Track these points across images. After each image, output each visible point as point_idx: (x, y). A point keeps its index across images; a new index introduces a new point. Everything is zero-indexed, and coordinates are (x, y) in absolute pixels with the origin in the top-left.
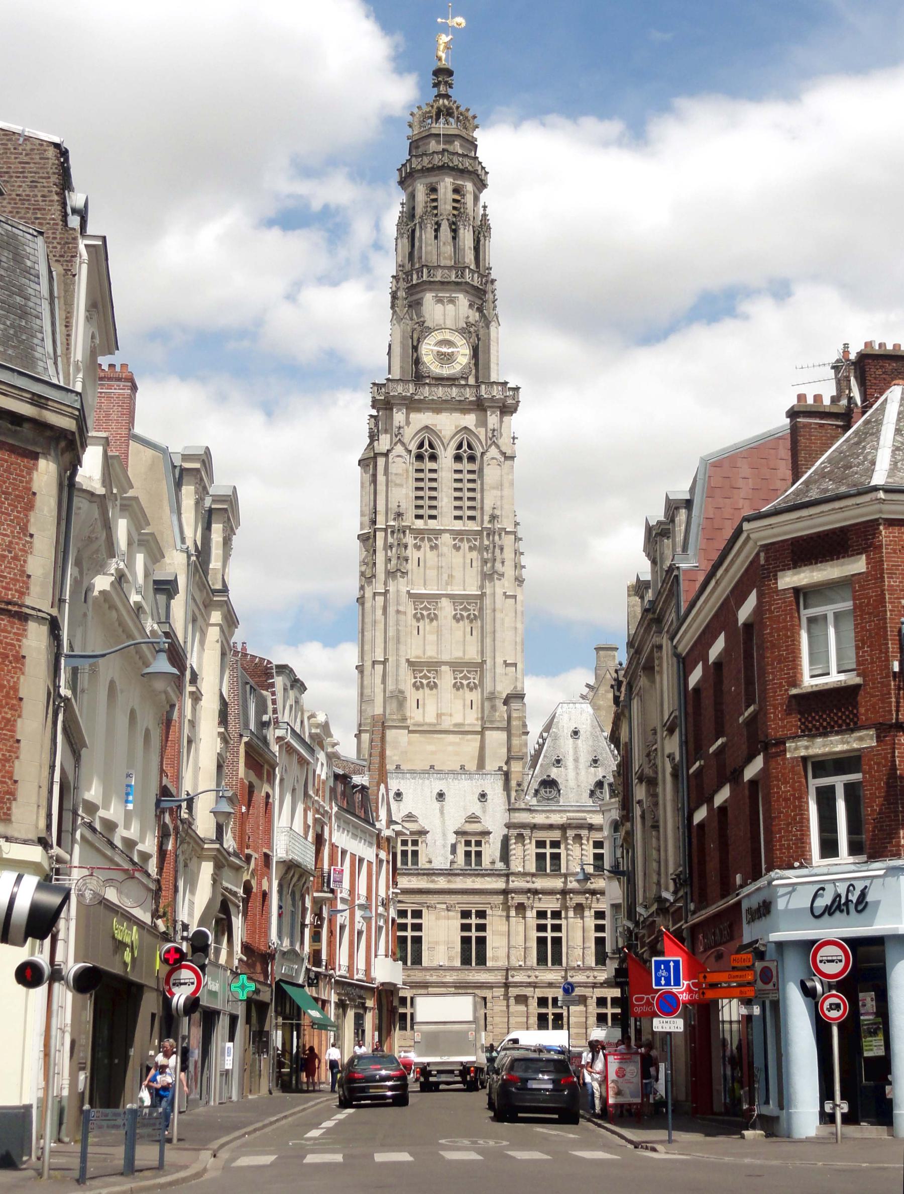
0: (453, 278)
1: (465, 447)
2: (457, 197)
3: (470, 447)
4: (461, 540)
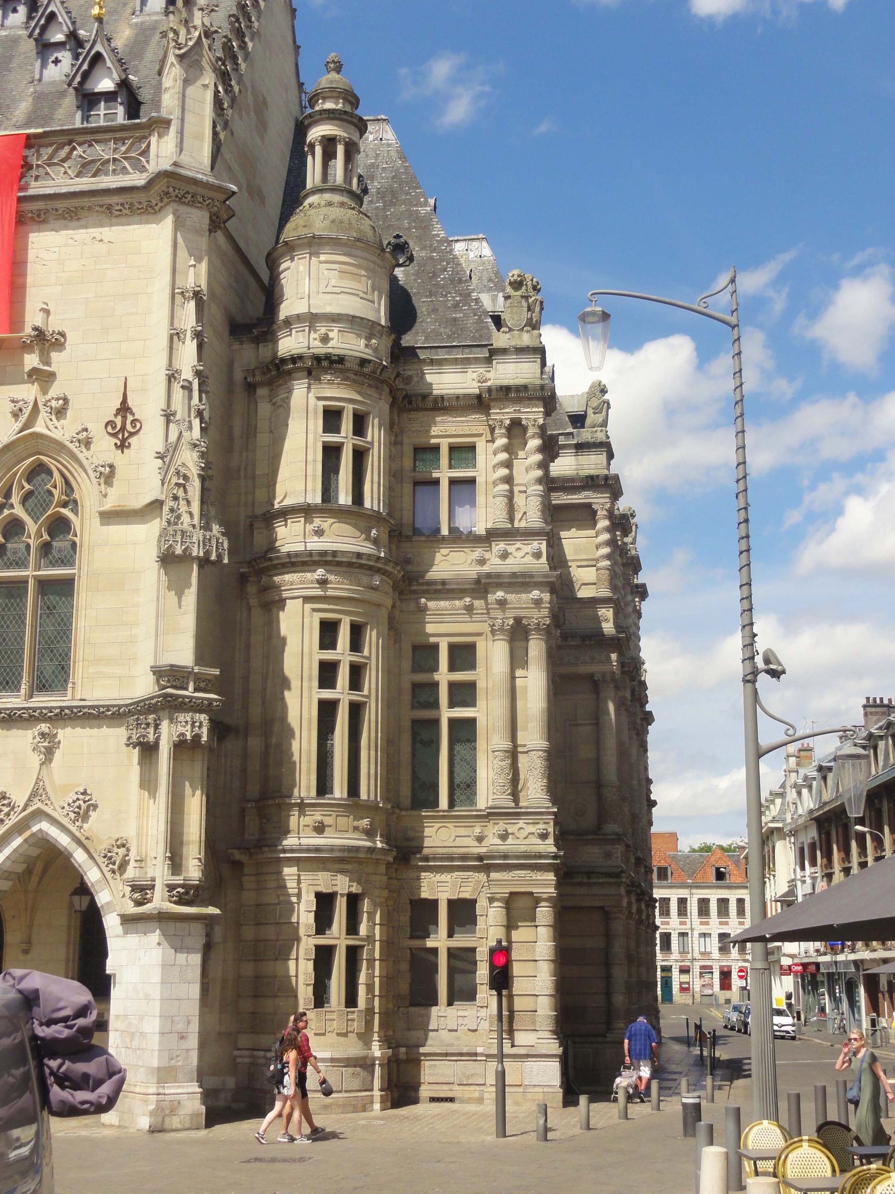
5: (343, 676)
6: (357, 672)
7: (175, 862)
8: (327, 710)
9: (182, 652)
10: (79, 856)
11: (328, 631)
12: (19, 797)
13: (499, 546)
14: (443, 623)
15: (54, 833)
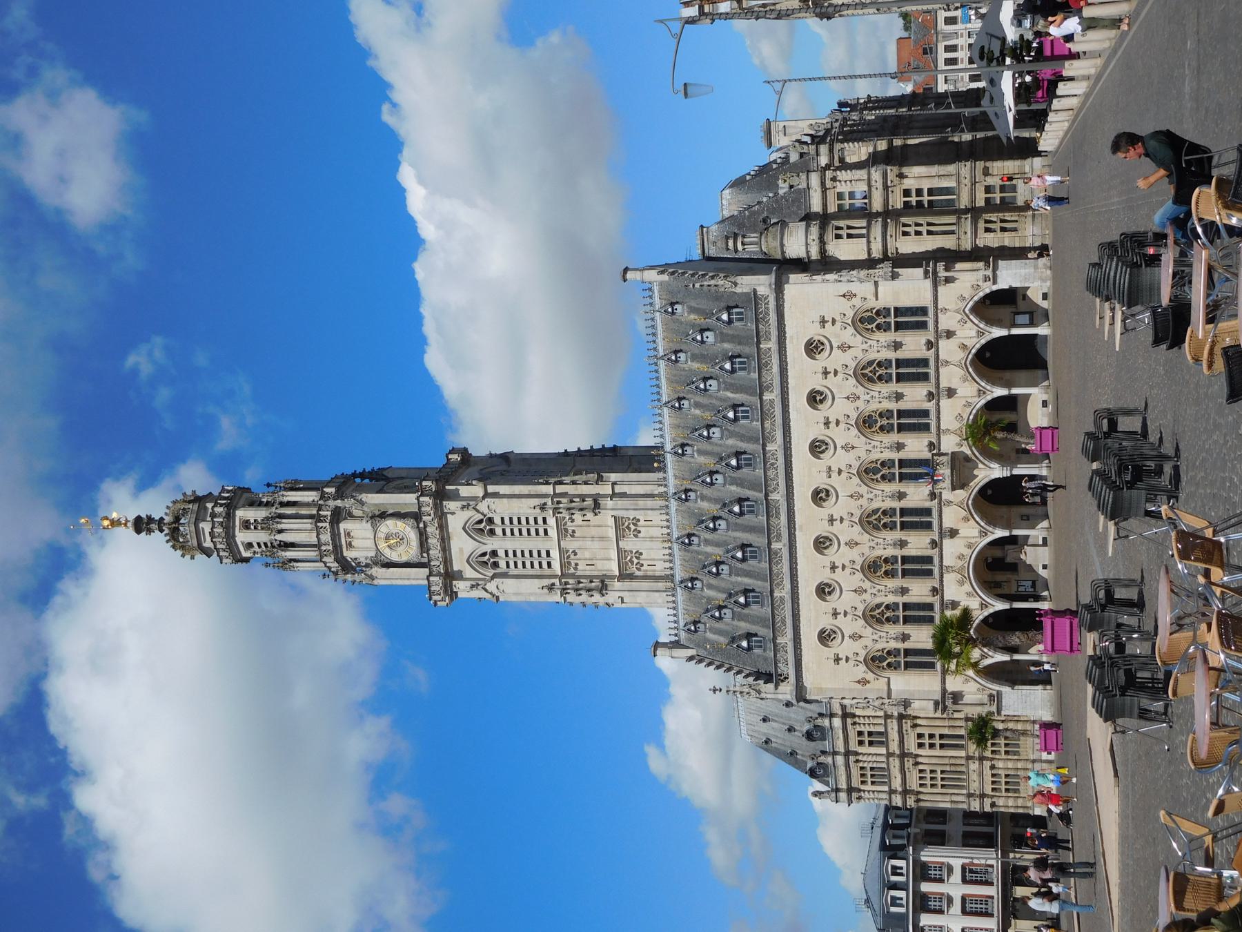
3: (480, 522)
4: (566, 530)
5: (919, 229)
6: (917, 225)
8: (929, 233)
9: (919, 272)
10: (976, 298)
11: (905, 234)
12: (959, 317)
13: (873, 183)
14: (897, 202)
15: (969, 306)
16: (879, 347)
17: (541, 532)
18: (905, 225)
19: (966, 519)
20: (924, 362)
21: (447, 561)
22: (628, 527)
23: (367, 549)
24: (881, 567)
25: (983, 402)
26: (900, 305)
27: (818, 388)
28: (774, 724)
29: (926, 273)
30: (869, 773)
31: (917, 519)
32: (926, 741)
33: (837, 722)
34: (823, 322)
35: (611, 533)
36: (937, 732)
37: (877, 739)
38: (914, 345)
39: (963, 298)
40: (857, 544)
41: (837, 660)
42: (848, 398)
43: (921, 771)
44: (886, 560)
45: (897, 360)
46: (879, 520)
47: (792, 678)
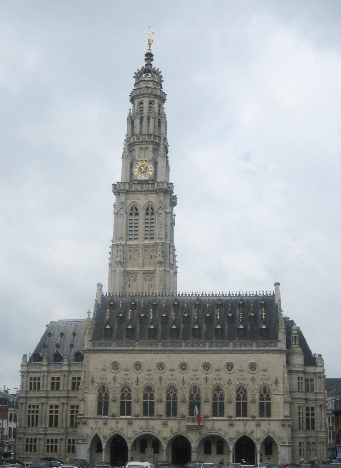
0: (147, 140)
1: (150, 209)
2: (150, 106)
3: (152, 209)
7: (289, 440)
9: (288, 414)
10: (274, 438)
16: (253, 395)
17: (146, 236)
18: (302, 407)
19: (172, 431)
20: (245, 415)
21: (135, 192)
22: (148, 276)
23: (139, 157)
24: (149, 392)
25: (227, 440)
26: (272, 405)
27: (235, 367)
28: (60, 338)
29: (288, 417)
30: (37, 381)
31: (172, 409)
32: (54, 409)
33: (65, 368)
34: (265, 371)
35: (146, 269)
36: (59, 414)
37: (55, 386)
38: (254, 409)
39: (275, 432)
40: (160, 381)
41: (104, 370)
42: (230, 380)
43: (37, 406)
44: (152, 395)
45: (246, 403)
46: (172, 392)
47: (94, 348)
